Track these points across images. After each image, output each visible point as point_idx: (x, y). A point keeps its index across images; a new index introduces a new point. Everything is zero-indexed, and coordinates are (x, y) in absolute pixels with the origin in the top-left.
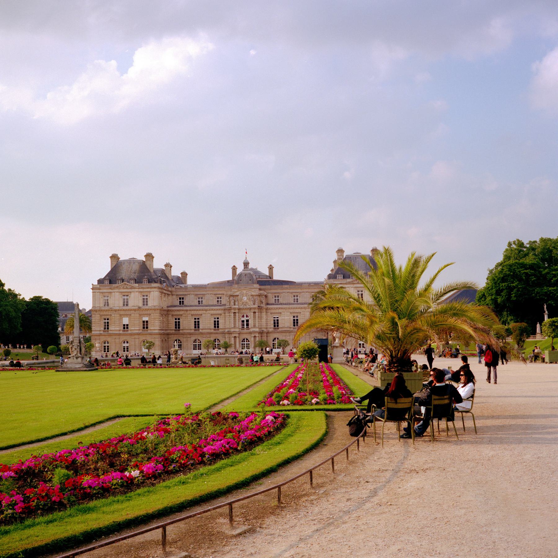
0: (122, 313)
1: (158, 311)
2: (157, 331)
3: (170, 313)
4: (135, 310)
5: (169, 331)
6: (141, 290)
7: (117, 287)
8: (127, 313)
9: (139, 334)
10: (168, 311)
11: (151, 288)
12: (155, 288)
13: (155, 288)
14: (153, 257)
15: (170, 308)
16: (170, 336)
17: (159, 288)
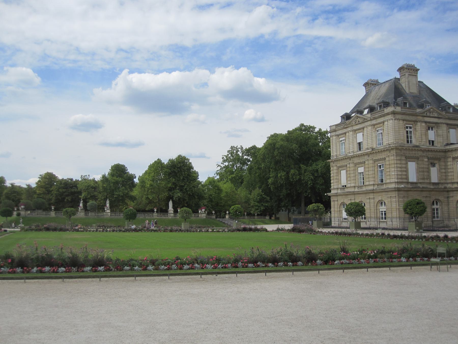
0: (356, 160)
1: (394, 152)
2: (393, 186)
3: (449, 154)
4: (368, 154)
5: (449, 186)
6: (374, 122)
7: (350, 124)
8: (361, 160)
9: (373, 192)
10: (445, 151)
11: (384, 116)
12: (388, 114)
13: (388, 114)
14: (418, 70)
15: (448, 147)
16: (451, 194)
17: (394, 113)
